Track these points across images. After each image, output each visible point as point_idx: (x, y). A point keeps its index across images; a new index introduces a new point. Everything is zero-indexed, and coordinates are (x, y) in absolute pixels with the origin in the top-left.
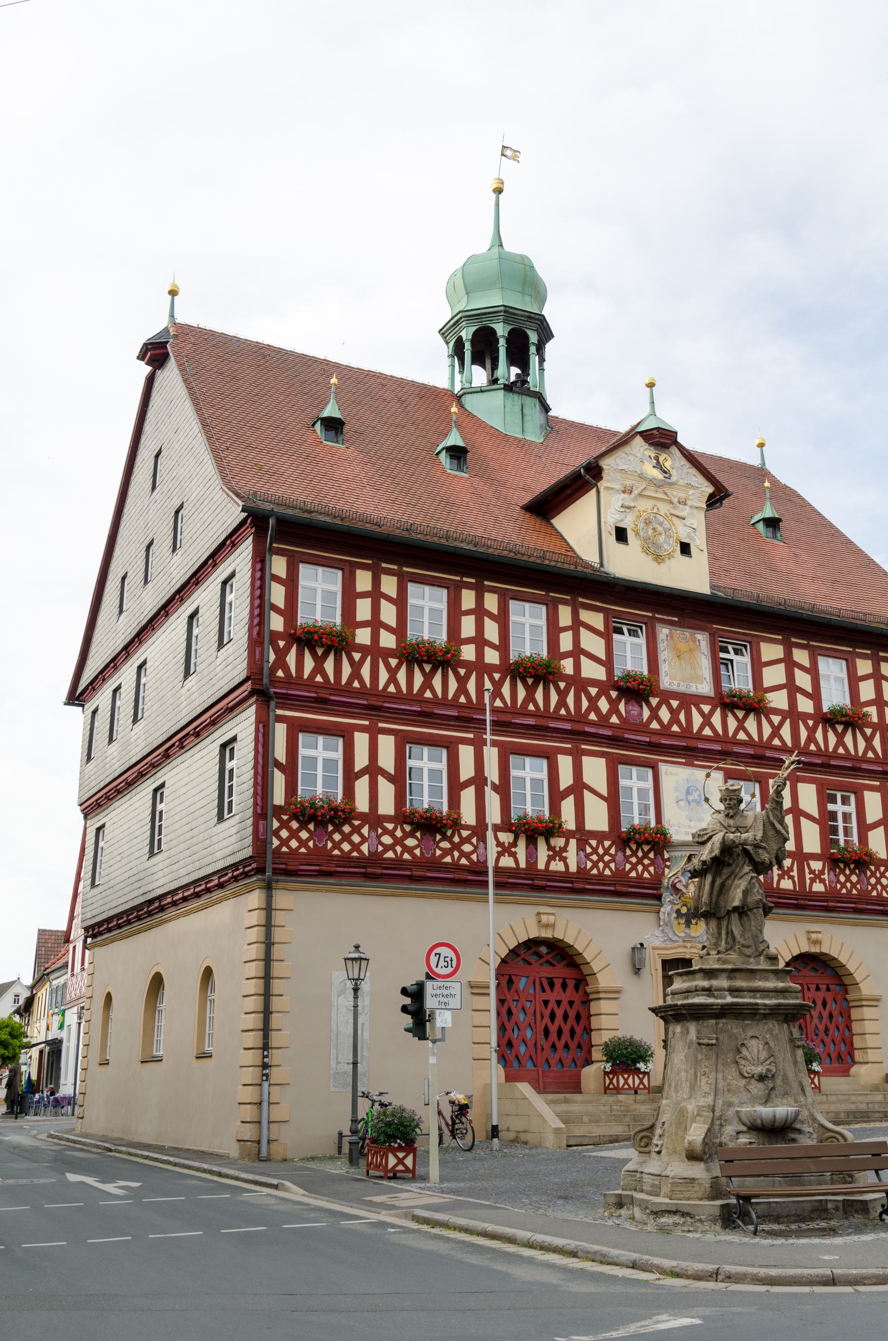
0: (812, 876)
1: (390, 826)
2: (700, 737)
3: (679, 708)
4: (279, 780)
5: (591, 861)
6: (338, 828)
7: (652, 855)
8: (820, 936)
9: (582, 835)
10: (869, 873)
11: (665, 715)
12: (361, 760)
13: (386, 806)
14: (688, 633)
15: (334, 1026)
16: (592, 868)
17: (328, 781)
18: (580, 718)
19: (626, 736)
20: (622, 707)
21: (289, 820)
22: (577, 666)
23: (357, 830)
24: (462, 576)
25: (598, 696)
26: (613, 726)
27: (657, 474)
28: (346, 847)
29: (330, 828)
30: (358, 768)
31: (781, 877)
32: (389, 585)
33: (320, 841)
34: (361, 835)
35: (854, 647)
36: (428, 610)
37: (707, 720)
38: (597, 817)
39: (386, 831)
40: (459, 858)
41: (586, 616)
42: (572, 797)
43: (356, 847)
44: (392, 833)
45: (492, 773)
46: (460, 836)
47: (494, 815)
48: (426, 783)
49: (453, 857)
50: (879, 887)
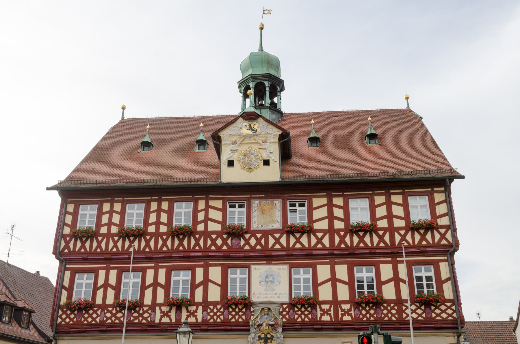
0: (343, 312)
1: (110, 309)
2: (273, 249)
3: (261, 238)
4: (64, 294)
5: (210, 316)
6: (87, 312)
7: (244, 310)
9: (205, 304)
10: (382, 308)
11: (253, 242)
13: (110, 300)
14: (269, 201)
16: (210, 319)
17: (184, 290)
18: (206, 249)
19: (231, 255)
20: (229, 242)
21: (67, 311)
22: (206, 227)
23: (95, 312)
25: (217, 238)
26: (224, 251)
27: (250, 132)
28: (90, 320)
29: (84, 312)
31: (322, 315)
32: (117, 207)
33: (79, 318)
34: (97, 314)
35: (373, 191)
36: (135, 214)
37: (277, 241)
39: (109, 311)
40: (142, 320)
41: (212, 203)
44: (111, 312)
46: (143, 310)
47: (160, 299)
48: (131, 288)
50: (390, 315)
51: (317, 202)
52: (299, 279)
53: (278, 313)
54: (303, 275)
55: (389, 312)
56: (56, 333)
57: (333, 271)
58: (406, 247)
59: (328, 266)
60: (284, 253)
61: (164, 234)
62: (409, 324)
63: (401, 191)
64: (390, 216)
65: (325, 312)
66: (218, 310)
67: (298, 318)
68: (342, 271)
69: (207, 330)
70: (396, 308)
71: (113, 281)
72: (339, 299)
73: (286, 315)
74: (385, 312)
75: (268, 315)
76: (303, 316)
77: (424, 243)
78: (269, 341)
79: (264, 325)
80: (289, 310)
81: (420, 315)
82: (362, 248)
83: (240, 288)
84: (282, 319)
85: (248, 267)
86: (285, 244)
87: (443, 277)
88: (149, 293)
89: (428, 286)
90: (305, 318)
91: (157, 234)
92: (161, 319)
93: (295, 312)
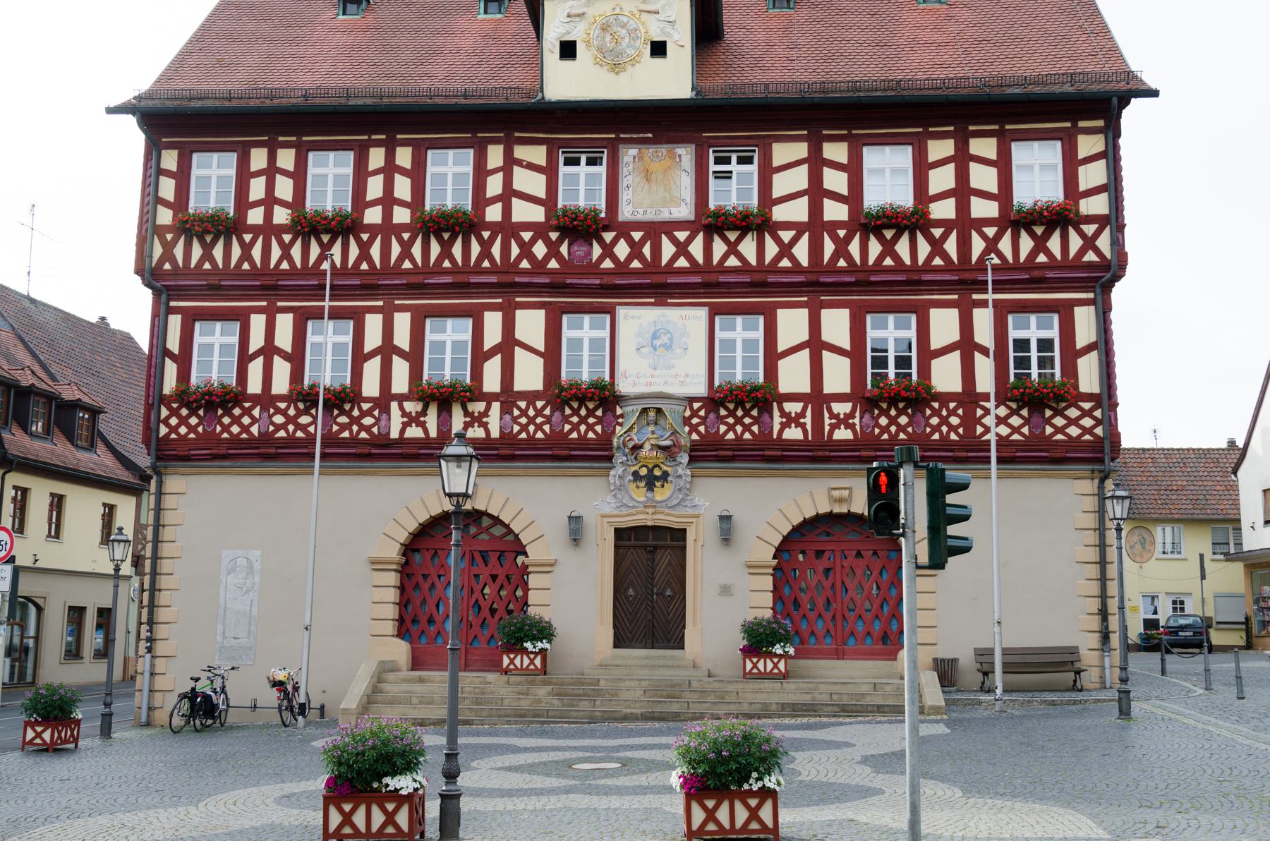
1: (283, 405)
2: (670, 269)
3: (643, 241)
4: (171, 369)
5: (519, 424)
6: (228, 412)
7: (599, 413)
8: (846, 493)
9: (508, 397)
10: (928, 412)
11: (622, 250)
12: (257, 341)
13: (281, 385)
14: (663, 149)
15: (222, 602)
16: (519, 432)
17: (456, 364)
18: (509, 267)
19: (568, 281)
20: (564, 249)
21: (179, 408)
22: (507, 211)
23: (247, 412)
24: (370, 133)
25: (533, 241)
26: (553, 272)
28: (235, 429)
29: (220, 412)
30: (367, 349)
31: (784, 426)
32: (286, 159)
34: (252, 417)
36: (330, 178)
37: (682, 249)
38: (530, 374)
39: (278, 411)
40: (358, 432)
41: (520, 152)
42: (499, 356)
43: (245, 429)
44: (284, 413)
45: (402, 338)
46: (360, 409)
47: (400, 383)
48: (329, 358)
49: (351, 432)
50: (944, 429)
51: (783, 152)
52: (733, 341)
53: (681, 421)
54: (742, 333)
55: (944, 421)
56: (158, 458)
57: (815, 325)
58: (995, 269)
59: (804, 313)
60: (697, 279)
61: (403, 227)
62: (989, 450)
63: (997, 127)
64: (963, 192)
65: (790, 420)
66: (539, 413)
67: (726, 432)
68: (836, 324)
69: (513, 458)
70: (960, 412)
71: (284, 339)
72: (828, 389)
73: (699, 424)
74: (935, 421)
75: (656, 424)
76: (739, 429)
77: (1042, 258)
78: (658, 484)
79: (647, 446)
80: (707, 413)
81: (1016, 430)
82: (888, 270)
83: (590, 362)
84: (690, 433)
85: (611, 311)
86: (699, 257)
87: (1081, 343)
88: (372, 369)
89: (1042, 363)
90: (743, 433)
91: (387, 229)
92: (402, 431)
93: (721, 420)
